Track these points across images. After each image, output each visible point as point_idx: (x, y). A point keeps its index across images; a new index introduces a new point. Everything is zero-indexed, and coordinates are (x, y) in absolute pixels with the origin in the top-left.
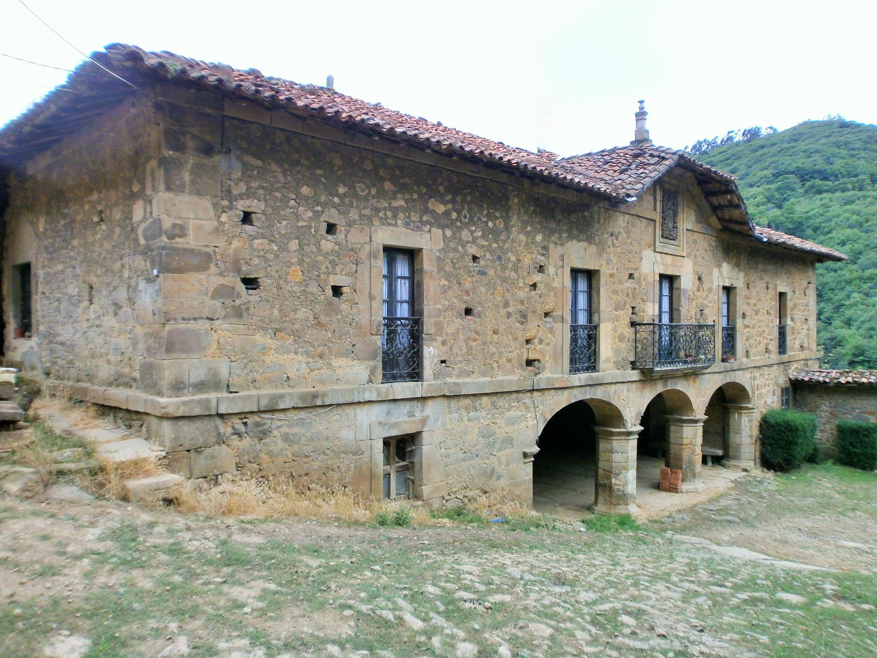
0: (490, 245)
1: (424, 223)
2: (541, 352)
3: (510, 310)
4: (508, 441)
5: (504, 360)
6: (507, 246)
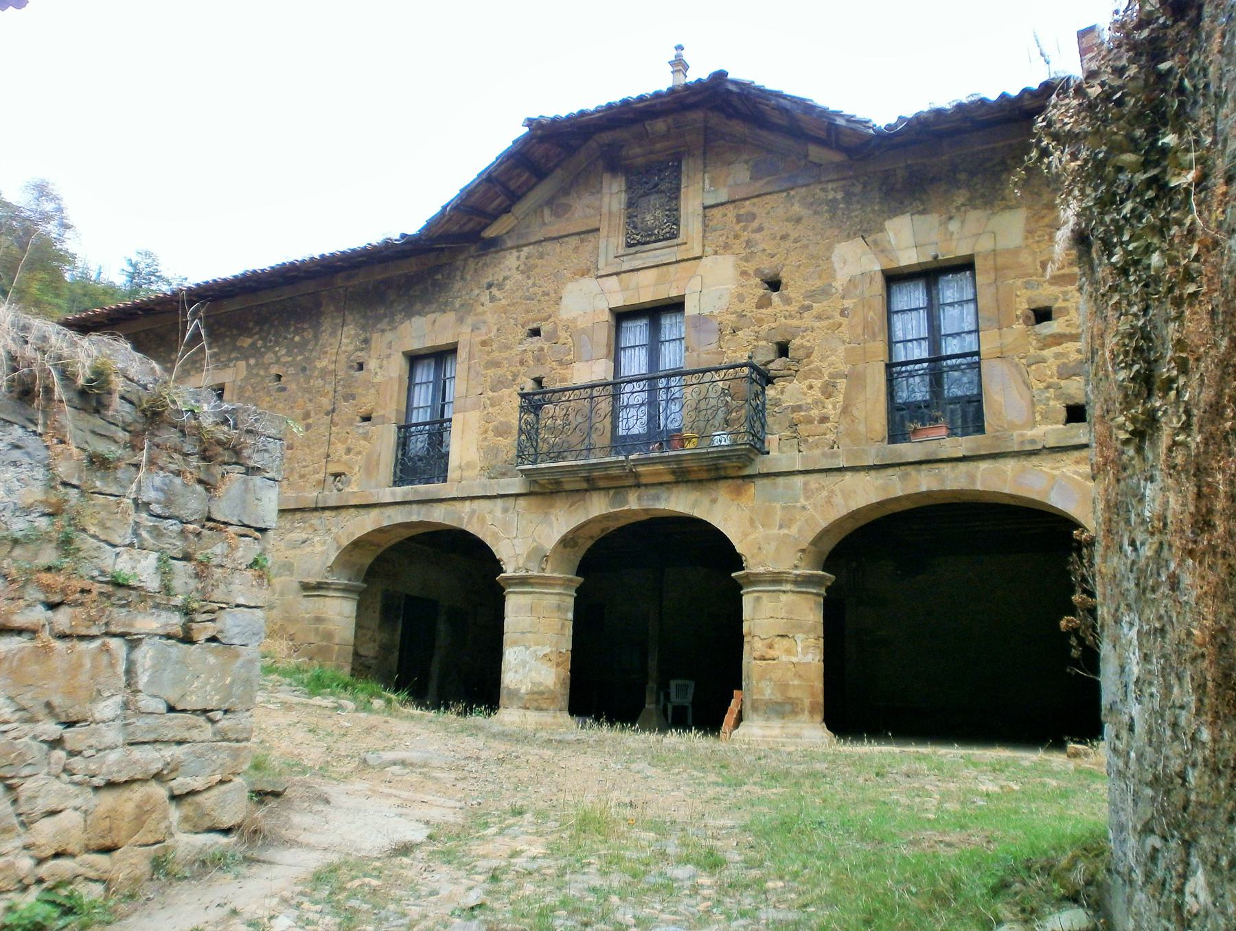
0: (294, 359)
1: (230, 360)
2: (346, 463)
3: (310, 421)
5: (296, 477)
6: (314, 354)
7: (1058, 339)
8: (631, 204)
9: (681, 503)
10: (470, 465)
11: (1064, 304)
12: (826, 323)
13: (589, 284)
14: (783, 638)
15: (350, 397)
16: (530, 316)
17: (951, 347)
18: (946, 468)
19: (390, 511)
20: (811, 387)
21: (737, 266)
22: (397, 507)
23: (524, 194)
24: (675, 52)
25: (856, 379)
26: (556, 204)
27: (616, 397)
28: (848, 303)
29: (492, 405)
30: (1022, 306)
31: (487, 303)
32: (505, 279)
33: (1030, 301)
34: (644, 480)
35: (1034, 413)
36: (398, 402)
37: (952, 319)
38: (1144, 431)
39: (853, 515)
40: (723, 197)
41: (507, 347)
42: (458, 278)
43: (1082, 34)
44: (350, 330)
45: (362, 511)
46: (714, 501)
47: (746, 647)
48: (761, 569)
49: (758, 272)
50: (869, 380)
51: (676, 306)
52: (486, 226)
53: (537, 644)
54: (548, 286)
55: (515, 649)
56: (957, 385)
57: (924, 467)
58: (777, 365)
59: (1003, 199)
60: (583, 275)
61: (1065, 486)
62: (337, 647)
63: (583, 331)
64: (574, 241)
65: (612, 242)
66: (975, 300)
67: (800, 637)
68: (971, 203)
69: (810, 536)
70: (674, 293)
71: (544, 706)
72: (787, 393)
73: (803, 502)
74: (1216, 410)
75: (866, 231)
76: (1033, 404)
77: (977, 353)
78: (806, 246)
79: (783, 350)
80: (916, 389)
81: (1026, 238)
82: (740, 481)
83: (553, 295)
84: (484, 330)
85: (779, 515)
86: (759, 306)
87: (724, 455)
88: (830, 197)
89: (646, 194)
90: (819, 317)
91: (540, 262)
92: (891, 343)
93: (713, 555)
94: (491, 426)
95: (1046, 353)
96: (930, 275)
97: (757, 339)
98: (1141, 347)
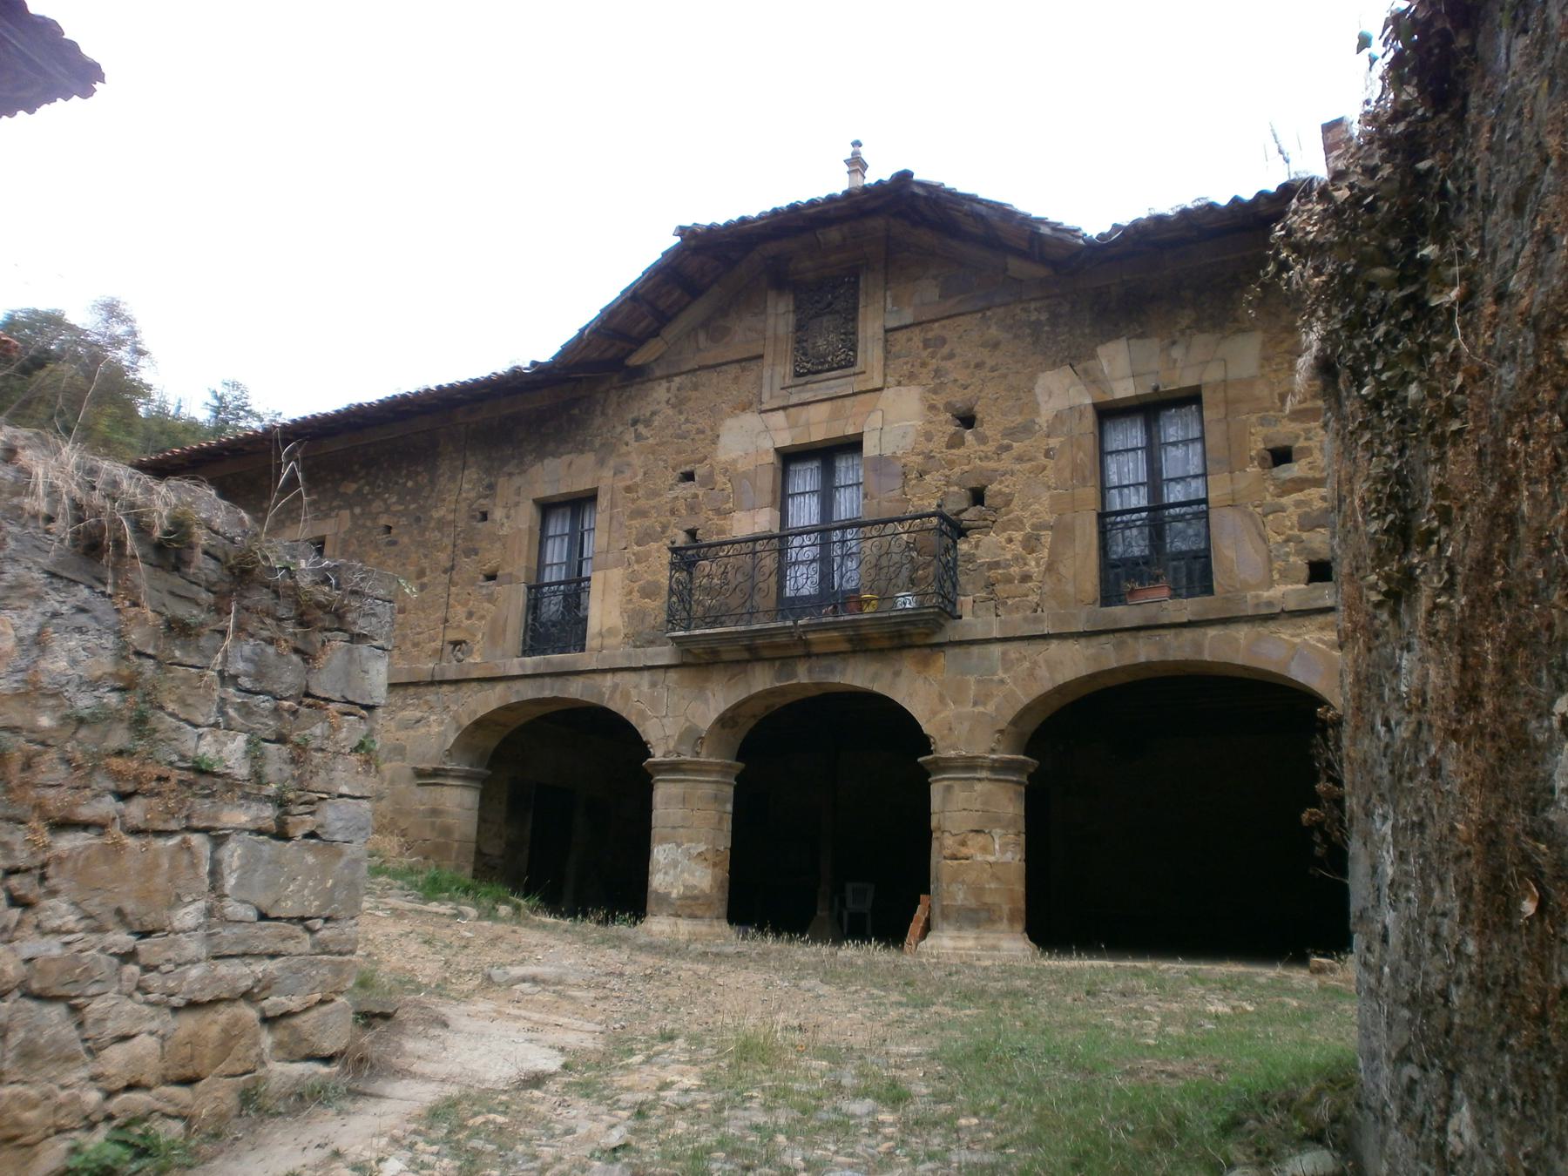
1: (332, 509)
3: (425, 580)
4: (399, 751)
7: (1300, 484)
8: (800, 327)
9: (857, 676)
10: (612, 631)
11: (1306, 444)
12: (1028, 465)
13: (750, 420)
14: (978, 834)
15: (471, 552)
16: (683, 457)
17: (1175, 493)
18: (1169, 635)
19: (518, 685)
20: (1010, 540)
21: (923, 399)
22: (527, 681)
23: (675, 315)
24: (852, 149)
25: (1063, 531)
26: (713, 326)
27: (782, 552)
28: (1054, 442)
29: (638, 562)
30: (1257, 446)
31: (632, 442)
32: (653, 413)
33: (1266, 439)
34: (815, 649)
35: (1271, 571)
36: (528, 558)
37: (1177, 460)
38: (1399, 592)
39: (1060, 690)
40: (908, 321)
41: (655, 494)
42: (598, 413)
43: (1328, 128)
44: (472, 473)
45: (486, 686)
46: (897, 674)
47: (935, 845)
48: (952, 753)
49: (949, 406)
50: (1078, 533)
51: (853, 445)
52: (631, 352)
53: (691, 841)
54: (703, 423)
55: (666, 846)
56: (1180, 540)
57: (1142, 634)
58: (970, 515)
59: (1236, 320)
60: (744, 410)
61: (1309, 655)
62: (456, 845)
63: (745, 475)
64: (733, 370)
65: (778, 371)
66: (1202, 439)
67: (997, 832)
68: (1198, 326)
69: (1010, 714)
70: (850, 431)
71: (699, 913)
72: (983, 547)
73: (1001, 674)
74: (1483, 567)
75: (1076, 358)
76: (1270, 561)
77: (1205, 501)
78: (1005, 376)
79: (978, 496)
80: (1134, 543)
81: (1262, 366)
82: (927, 651)
83: (709, 432)
84: (628, 473)
85: (973, 690)
86: (950, 446)
87: (909, 619)
88: (1033, 318)
89: (817, 315)
90: (1020, 459)
91: (694, 394)
92: (1104, 489)
93: (899, 735)
94: (636, 586)
95: (1284, 500)
96: (1149, 409)
97: (948, 484)
98: (1396, 495)
